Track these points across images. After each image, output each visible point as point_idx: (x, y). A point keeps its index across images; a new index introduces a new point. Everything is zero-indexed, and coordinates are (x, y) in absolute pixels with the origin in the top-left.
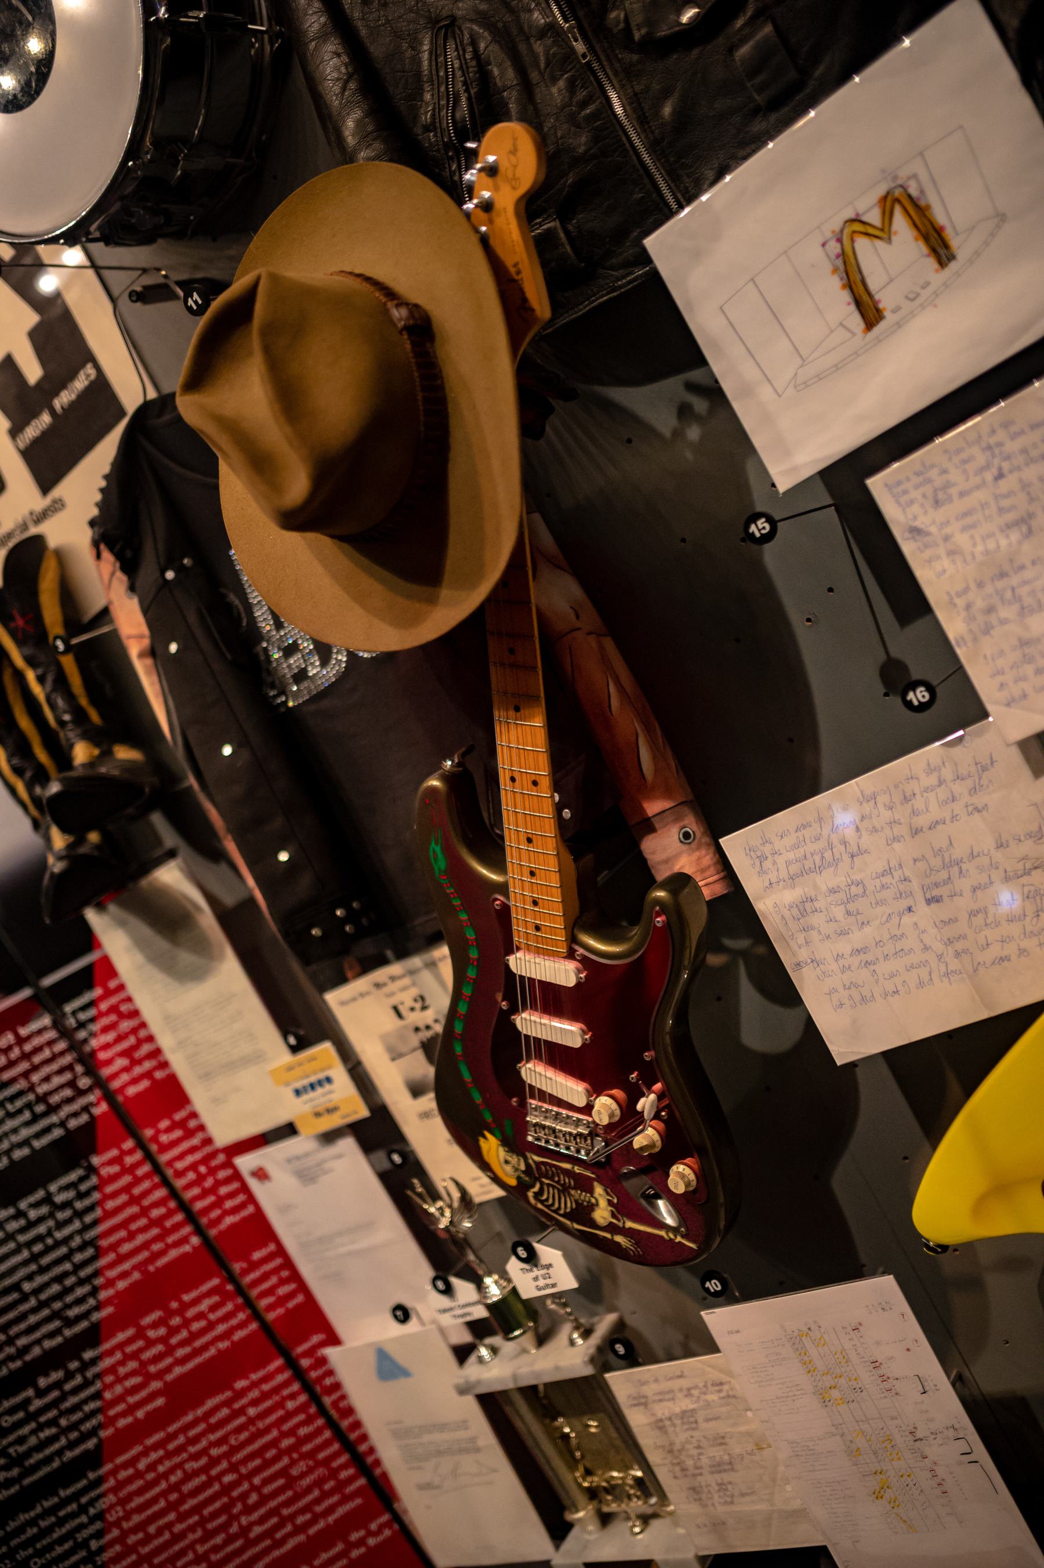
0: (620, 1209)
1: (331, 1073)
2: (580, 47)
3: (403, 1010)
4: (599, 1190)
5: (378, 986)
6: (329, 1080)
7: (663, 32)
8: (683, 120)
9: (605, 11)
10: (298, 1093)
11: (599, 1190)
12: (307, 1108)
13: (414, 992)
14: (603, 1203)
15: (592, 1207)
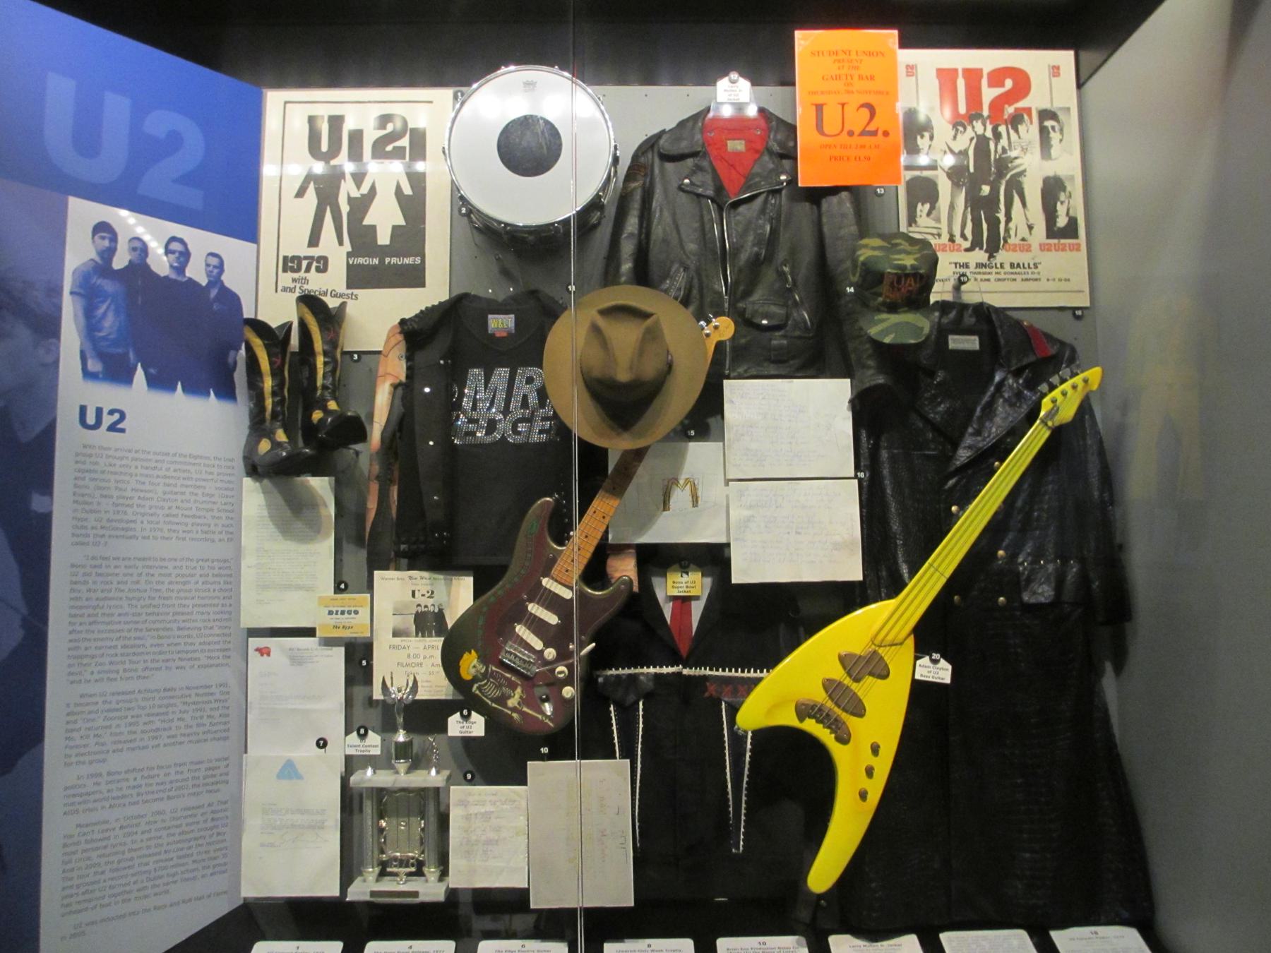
0: (523, 701)
1: (359, 609)
2: (726, 305)
3: (417, 594)
4: (519, 690)
5: (411, 578)
6: (356, 612)
7: (756, 320)
8: (746, 348)
9: (738, 301)
10: (330, 613)
11: (519, 690)
12: (332, 622)
13: (429, 588)
14: (517, 696)
15: (509, 697)
